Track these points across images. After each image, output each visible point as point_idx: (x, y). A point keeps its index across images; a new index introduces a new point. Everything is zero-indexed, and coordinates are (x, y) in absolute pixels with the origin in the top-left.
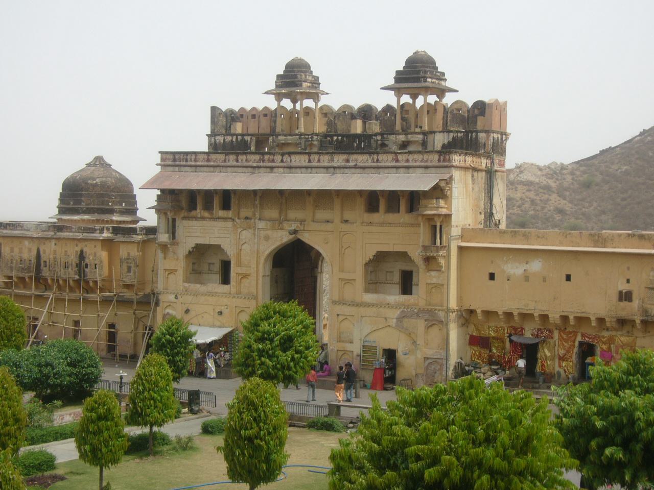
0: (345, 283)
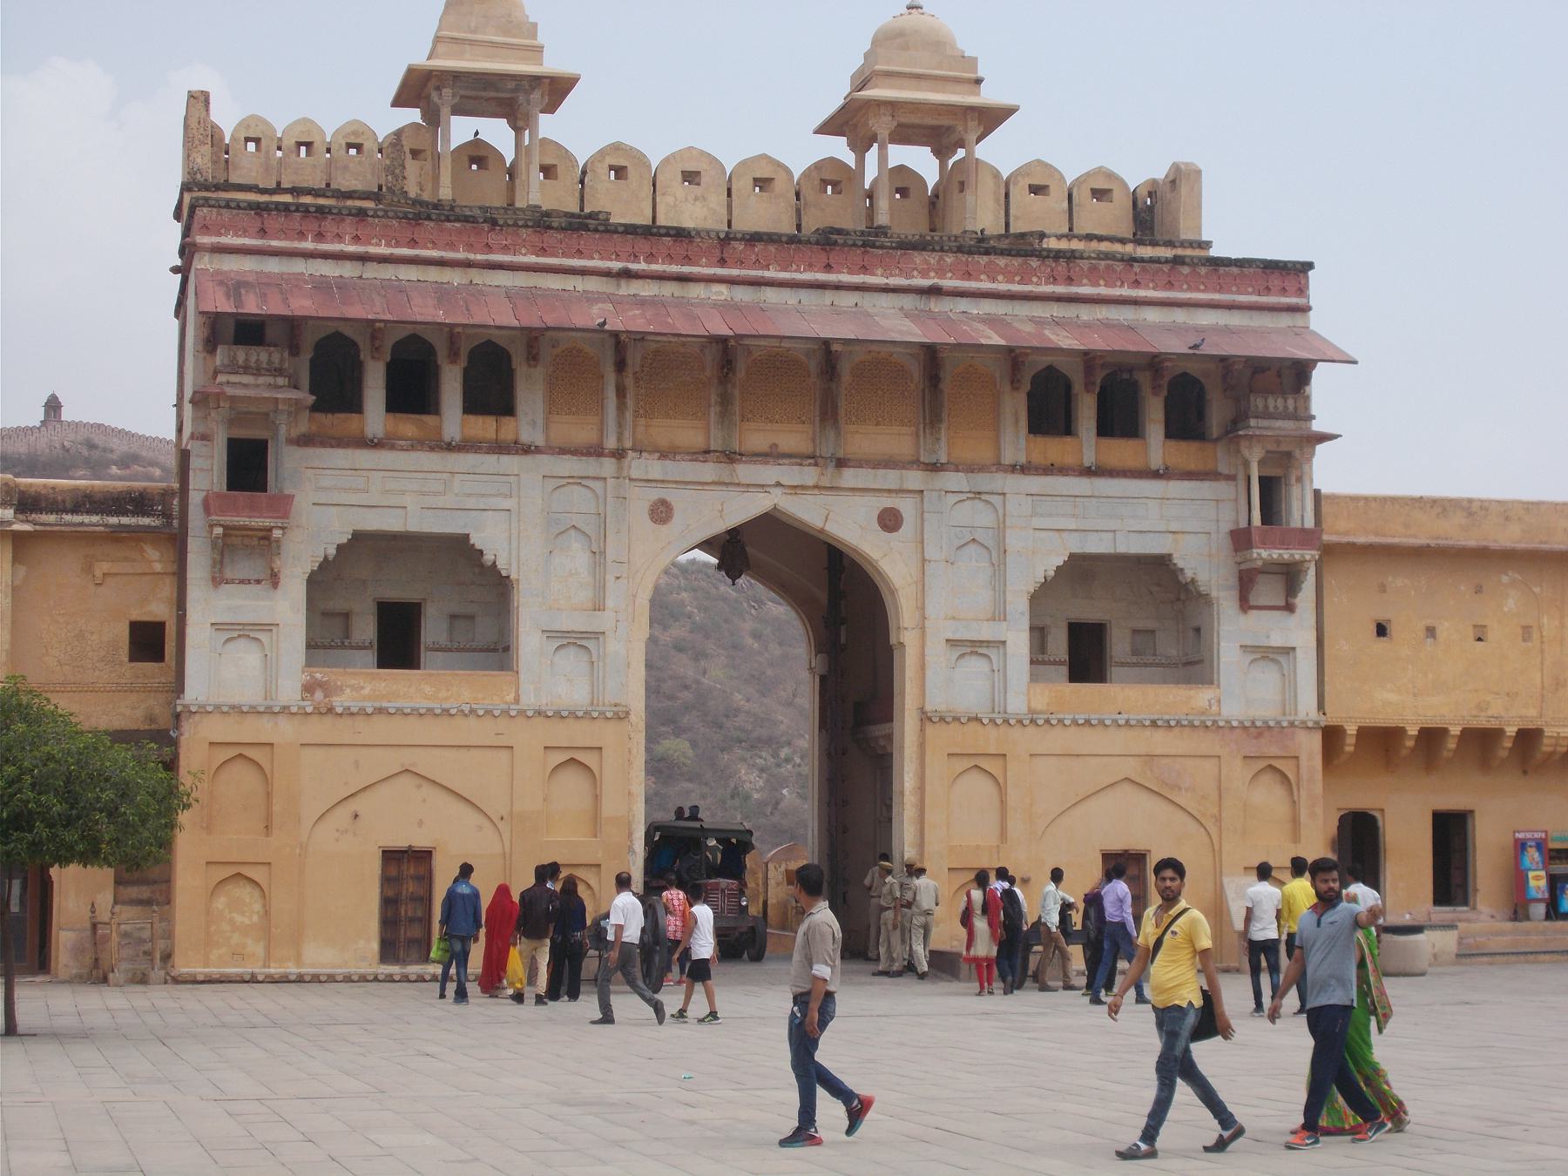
0: (963, 655)
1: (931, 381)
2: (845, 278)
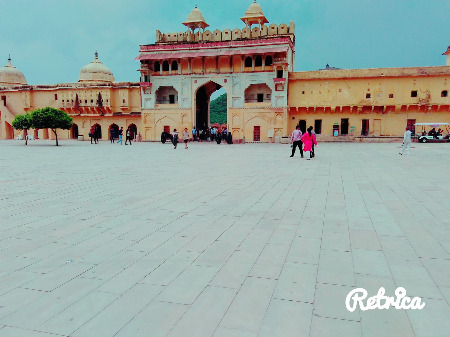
1: (231, 61)
2: (219, 47)
